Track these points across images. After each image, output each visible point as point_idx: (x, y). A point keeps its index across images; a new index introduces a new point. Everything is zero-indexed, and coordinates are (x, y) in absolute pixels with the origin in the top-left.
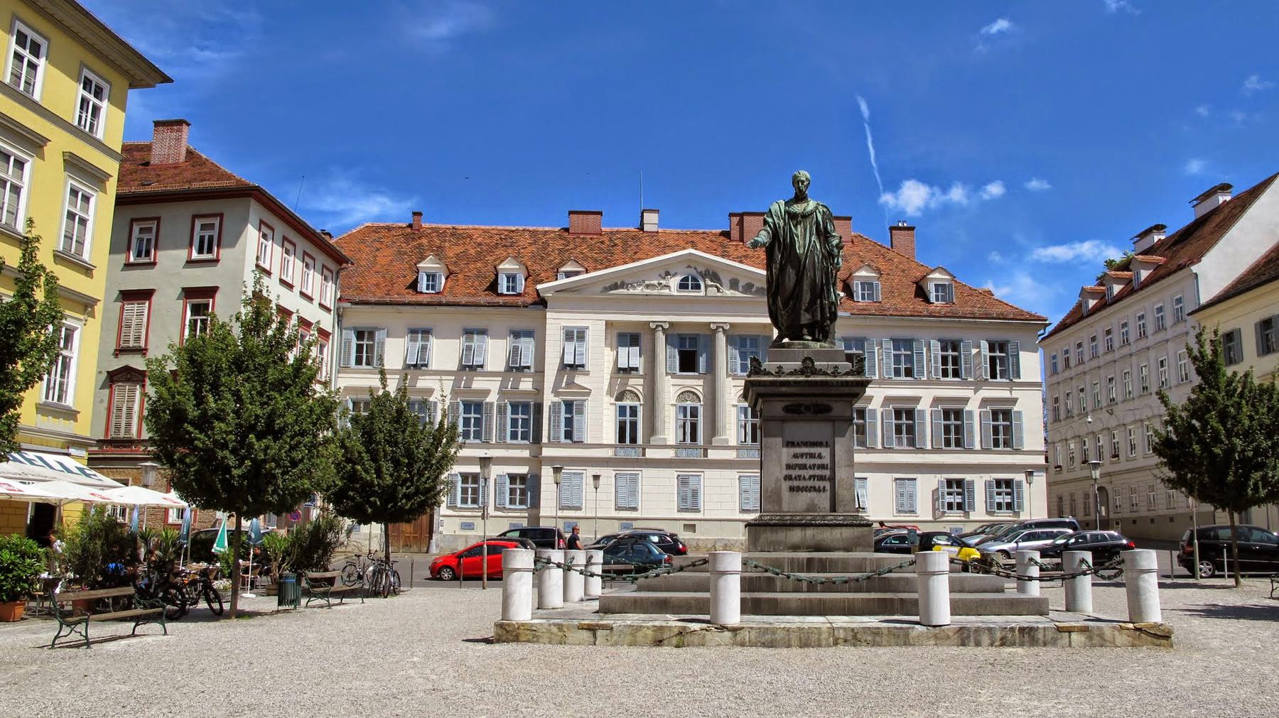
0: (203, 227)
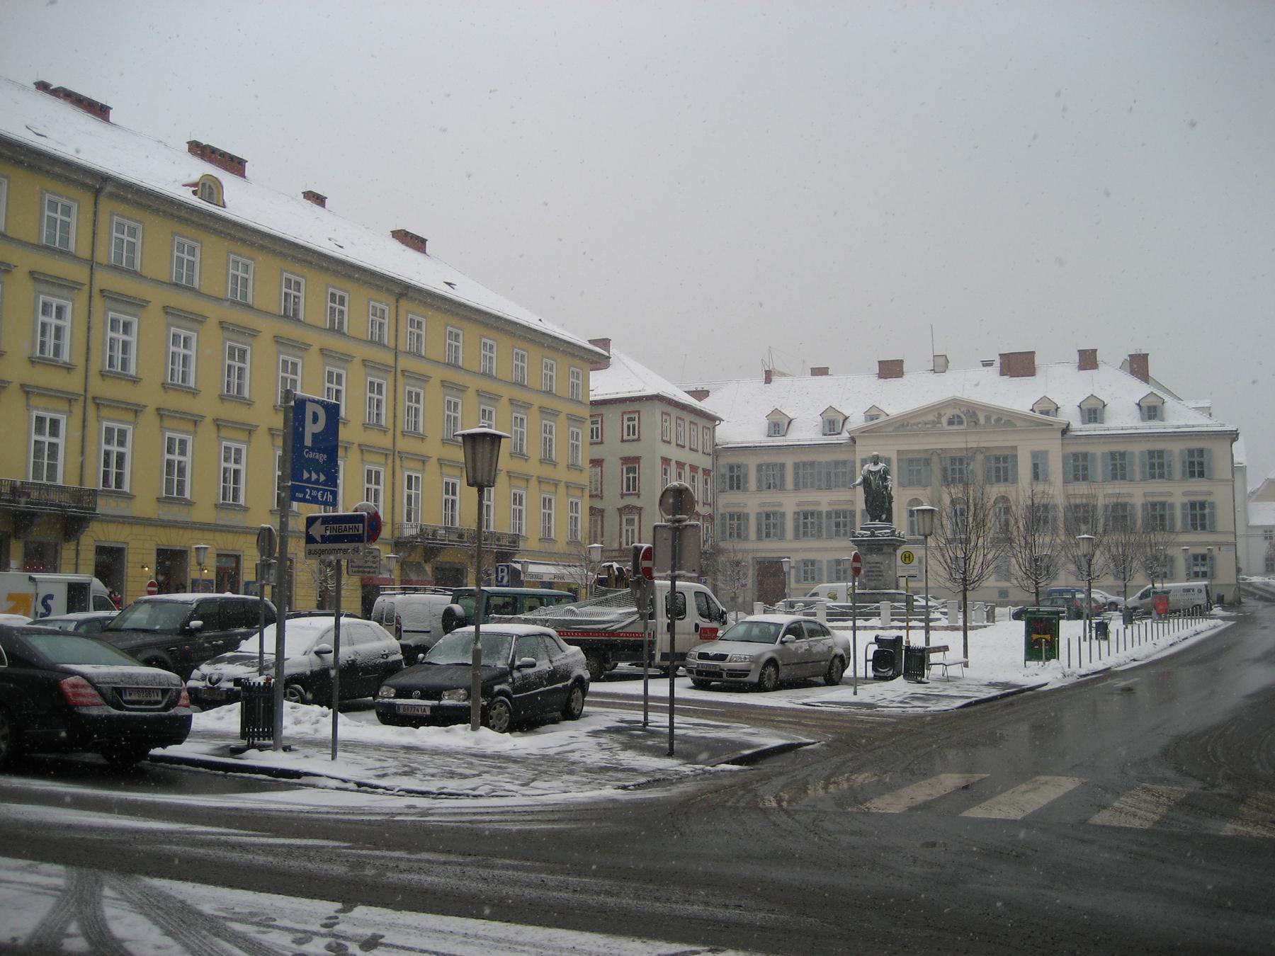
0: (629, 420)
